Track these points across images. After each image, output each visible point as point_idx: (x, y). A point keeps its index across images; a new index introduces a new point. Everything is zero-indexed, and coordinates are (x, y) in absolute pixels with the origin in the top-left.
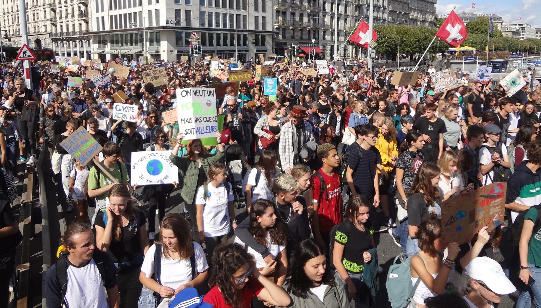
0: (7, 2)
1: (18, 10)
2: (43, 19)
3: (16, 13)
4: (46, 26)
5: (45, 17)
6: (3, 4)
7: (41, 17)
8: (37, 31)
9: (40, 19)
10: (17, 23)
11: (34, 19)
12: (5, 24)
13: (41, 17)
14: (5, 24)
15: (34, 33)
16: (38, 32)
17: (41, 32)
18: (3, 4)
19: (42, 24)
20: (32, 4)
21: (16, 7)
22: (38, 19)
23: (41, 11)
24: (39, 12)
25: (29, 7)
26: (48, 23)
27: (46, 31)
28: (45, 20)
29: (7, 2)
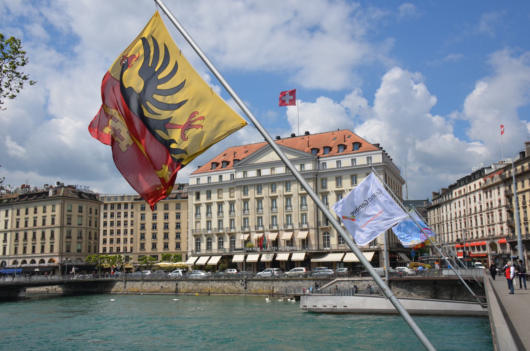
0: (460, 206)
1: (471, 213)
2: (499, 221)
3: (469, 216)
4: (502, 229)
5: (501, 220)
6: (455, 207)
7: (497, 219)
8: (492, 234)
9: (495, 222)
10: (470, 227)
11: (488, 222)
12: (457, 228)
13: (497, 219)
14: (457, 228)
15: (489, 236)
16: (493, 235)
17: (496, 235)
18: (455, 207)
19: (498, 228)
20: (486, 207)
21: (469, 209)
22: (493, 221)
23: (496, 213)
24: (494, 214)
25: (483, 209)
26: (505, 226)
27: (502, 234)
28: (501, 223)
29: (460, 206)
